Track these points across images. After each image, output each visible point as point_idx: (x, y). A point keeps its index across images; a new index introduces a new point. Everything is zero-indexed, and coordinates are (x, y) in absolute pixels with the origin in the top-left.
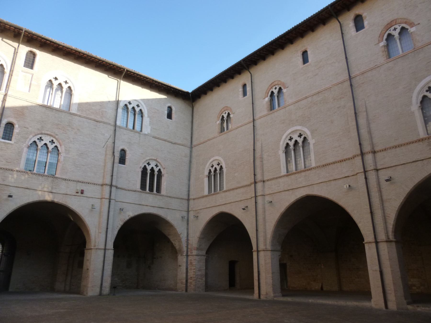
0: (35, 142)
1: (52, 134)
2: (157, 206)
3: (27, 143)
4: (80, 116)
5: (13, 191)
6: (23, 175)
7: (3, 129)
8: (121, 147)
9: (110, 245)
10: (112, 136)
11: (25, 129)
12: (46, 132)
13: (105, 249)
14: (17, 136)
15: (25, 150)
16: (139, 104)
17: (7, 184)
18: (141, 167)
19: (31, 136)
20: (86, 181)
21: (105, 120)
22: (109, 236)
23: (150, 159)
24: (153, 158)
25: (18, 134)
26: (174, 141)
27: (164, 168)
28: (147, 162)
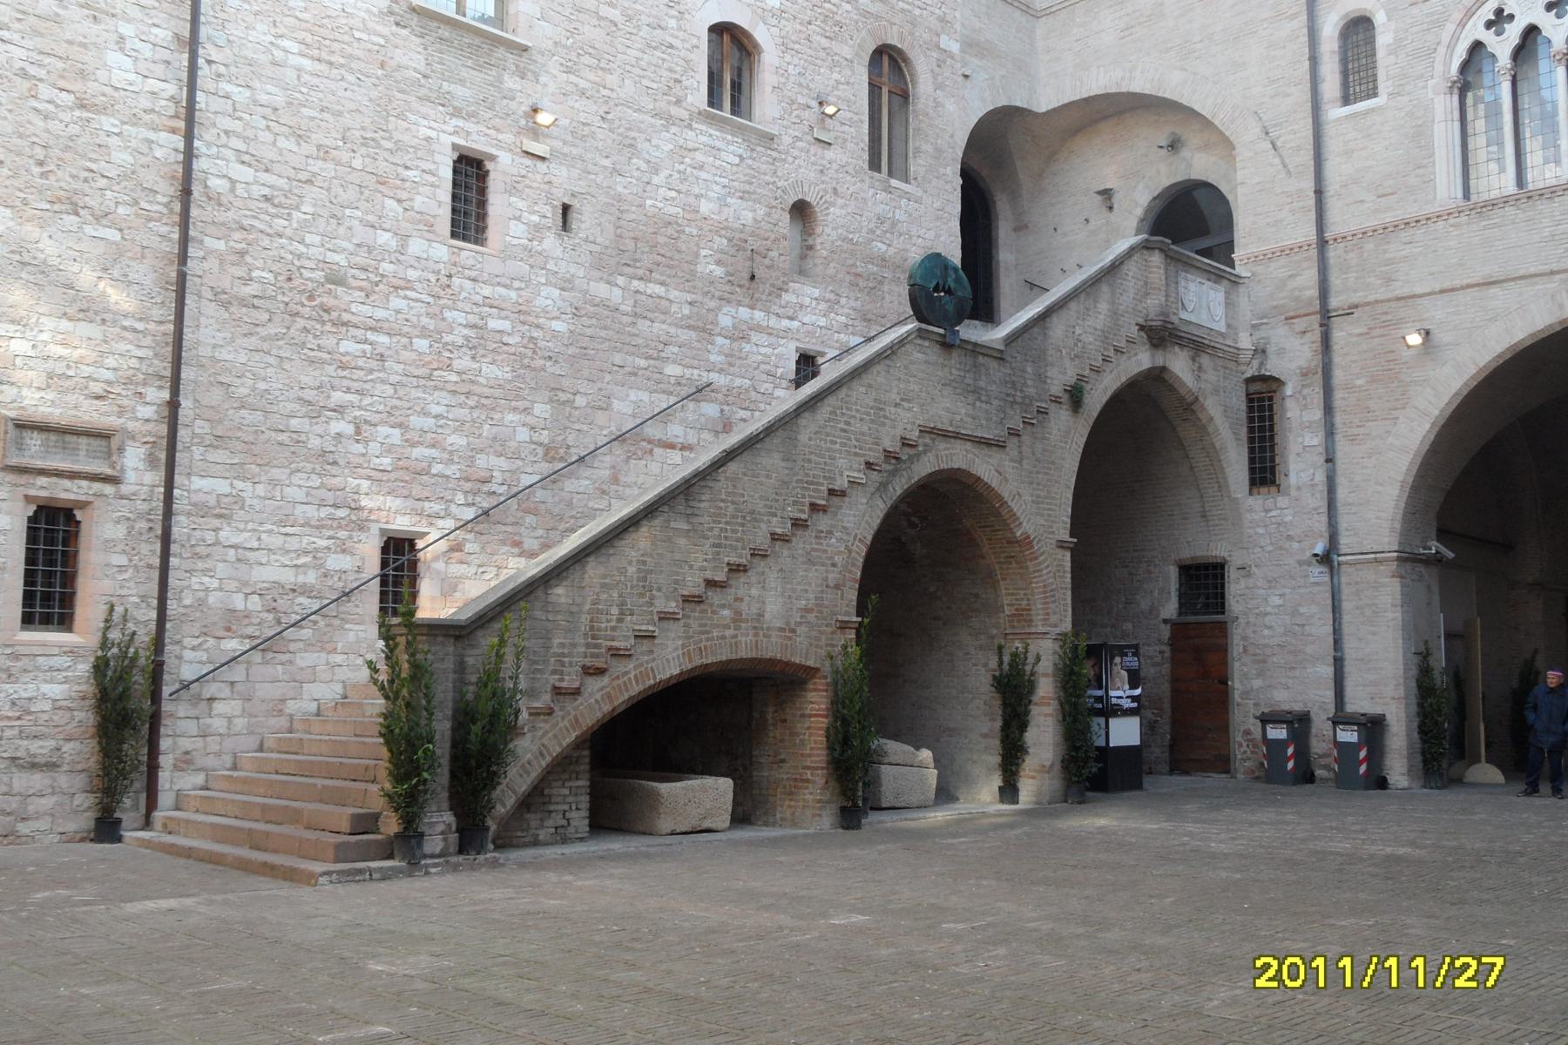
0: (1477, 46)
5: (1436, 313)
7: (1336, 58)
14: (1392, 59)
15: (1444, 106)
17: (1406, 291)
19: (1451, 27)
25: (1393, 51)
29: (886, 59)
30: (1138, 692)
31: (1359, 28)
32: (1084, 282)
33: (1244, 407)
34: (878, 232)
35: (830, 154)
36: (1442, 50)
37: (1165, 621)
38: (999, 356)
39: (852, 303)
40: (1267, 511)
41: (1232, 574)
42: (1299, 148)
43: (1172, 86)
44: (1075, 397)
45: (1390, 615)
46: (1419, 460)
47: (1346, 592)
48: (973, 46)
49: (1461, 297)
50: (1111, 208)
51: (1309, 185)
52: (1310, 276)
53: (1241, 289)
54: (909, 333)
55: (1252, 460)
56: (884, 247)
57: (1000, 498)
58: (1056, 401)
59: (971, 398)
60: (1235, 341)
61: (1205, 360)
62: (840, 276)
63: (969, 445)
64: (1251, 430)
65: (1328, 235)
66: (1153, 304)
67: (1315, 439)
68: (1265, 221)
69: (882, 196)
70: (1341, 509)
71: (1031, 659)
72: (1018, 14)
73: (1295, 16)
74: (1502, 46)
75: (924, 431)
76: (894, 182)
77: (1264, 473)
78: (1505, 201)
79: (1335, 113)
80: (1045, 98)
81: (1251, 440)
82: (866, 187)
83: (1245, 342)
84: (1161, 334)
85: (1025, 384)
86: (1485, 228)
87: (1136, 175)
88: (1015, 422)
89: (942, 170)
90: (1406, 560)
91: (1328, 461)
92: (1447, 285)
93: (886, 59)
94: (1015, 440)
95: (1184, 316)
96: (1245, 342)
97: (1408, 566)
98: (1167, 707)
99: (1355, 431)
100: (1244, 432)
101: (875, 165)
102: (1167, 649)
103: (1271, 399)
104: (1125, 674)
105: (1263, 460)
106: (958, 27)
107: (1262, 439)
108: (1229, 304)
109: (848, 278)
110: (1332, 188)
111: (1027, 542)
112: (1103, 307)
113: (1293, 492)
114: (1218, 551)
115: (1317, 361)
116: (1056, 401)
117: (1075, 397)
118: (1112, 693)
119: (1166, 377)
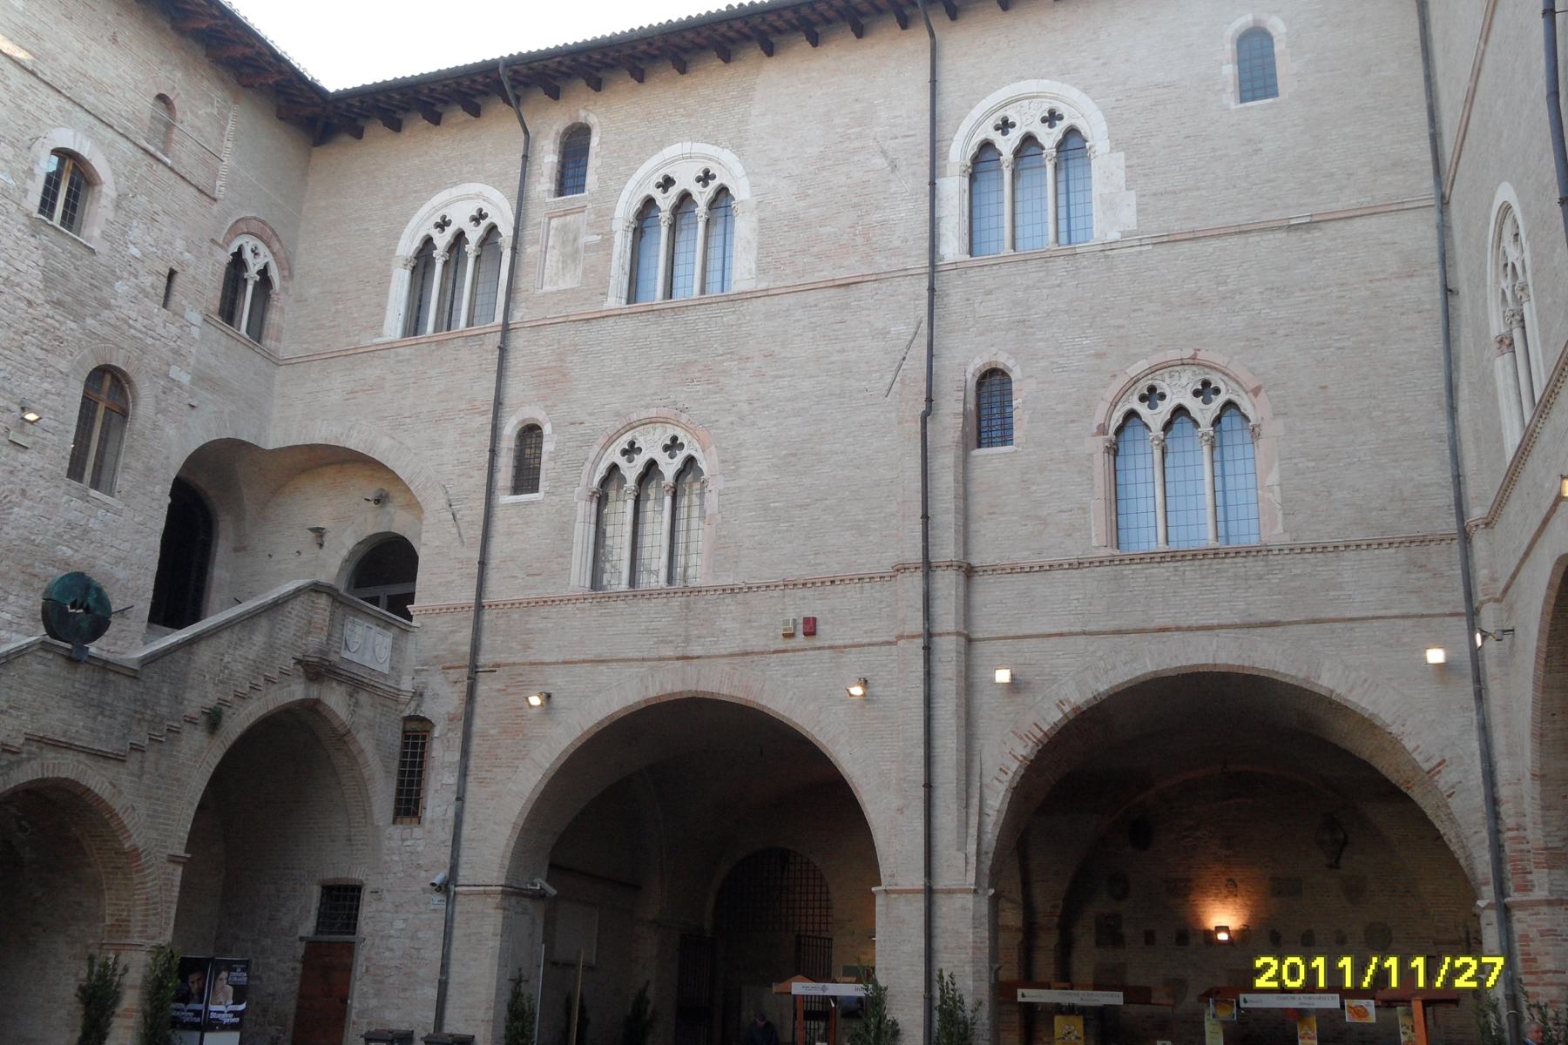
0: (614, 468)
1: (665, 412)
2: (1228, 617)
3: (584, 480)
4: (767, 294)
5: (558, 680)
6: (583, 610)
7: (512, 454)
8: (977, 365)
9: (959, 868)
10: (924, 325)
11: (572, 429)
12: (644, 414)
13: (929, 892)
14: (552, 464)
16: (1055, 104)
18: (1102, 430)
19: (596, 448)
20: (823, 572)
21: (882, 263)
22: (947, 819)
23: (1152, 371)
24: (1173, 355)
26: (1299, 216)
27: (1256, 391)
28: (1142, 388)
29: (108, 377)
30: (242, 1007)
31: (531, 433)
32: (241, 615)
33: (398, 742)
34: (66, 537)
35: (24, 457)
36: (588, 465)
37: (301, 939)
38: (133, 675)
39: (22, 602)
40: (403, 840)
41: (366, 896)
42: (473, 523)
43: (381, 449)
44: (213, 720)
45: (491, 944)
46: (529, 807)
47: (458, 919)
48: (203, 379)
49: (578, 669)
50: (321, 545)
51: (476, 555)
52: (466, 634)
53: (410, 637)
54: (30, 645)
55: (399, 792)
56: (69, 552)
57: (110, 810)
58: (192, 721)
59: (91, 712)
60: (398, 682)
61: (363, 697)
62: (12, 574)
63: (82, 757)
64: (403, 764)
65: (485, 601)
66: (314, 642)
67: (451, 779)
68: (440, 582)
69: (76, 503)
70: (464, 844)
71: (119, 971)
72: (258, 358)
73: (483, 413)
74: (631, 471)
75: (29, 739)
76: (93, 493)
77: (408, 805)
78: (618, 595)
79: (505, 499)
80: (273, 439)
81: (402, 773)
82: (60, 492)
83: (407, 684)
84: (318, 670)
85: (158, 704)
86: (601, 615)
87: (342, 523)
88: (141, 736)
89: (150, 488)
90: (512, 894)
91: (458, 799)
92: (568, 658)
93: (108, 377)
94: (139, 755)
95: (346, 655)
96: (407, 684)
97: (513, 900)
98: (290, 1023)
99: (484, 774)
100: (395, 765)
101: (75, 471)
102: (299, 966)
103: (424, 738)
104: (230, 989)
105: (409, 792)
106: (192, 361)
107: (412, 773)
108: (396, 649)
109: (21, 577)
110: (493, 562)
111: (135, 854)
112: (259, 639)
113: (428, 825)
114: (357, 874)
115: (461, 710)
116: (192, 721)
117: (213, 720)
118: (212, 1008)
119: (320, 708)
